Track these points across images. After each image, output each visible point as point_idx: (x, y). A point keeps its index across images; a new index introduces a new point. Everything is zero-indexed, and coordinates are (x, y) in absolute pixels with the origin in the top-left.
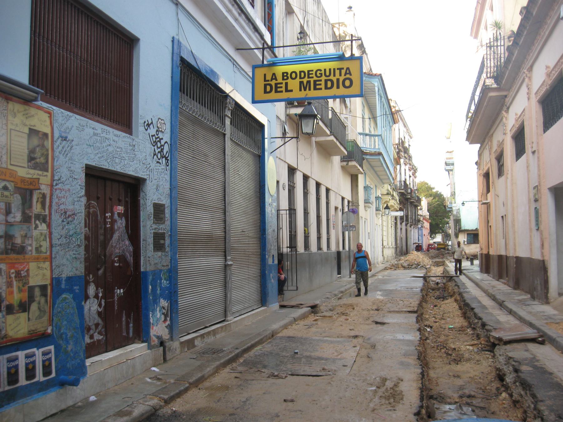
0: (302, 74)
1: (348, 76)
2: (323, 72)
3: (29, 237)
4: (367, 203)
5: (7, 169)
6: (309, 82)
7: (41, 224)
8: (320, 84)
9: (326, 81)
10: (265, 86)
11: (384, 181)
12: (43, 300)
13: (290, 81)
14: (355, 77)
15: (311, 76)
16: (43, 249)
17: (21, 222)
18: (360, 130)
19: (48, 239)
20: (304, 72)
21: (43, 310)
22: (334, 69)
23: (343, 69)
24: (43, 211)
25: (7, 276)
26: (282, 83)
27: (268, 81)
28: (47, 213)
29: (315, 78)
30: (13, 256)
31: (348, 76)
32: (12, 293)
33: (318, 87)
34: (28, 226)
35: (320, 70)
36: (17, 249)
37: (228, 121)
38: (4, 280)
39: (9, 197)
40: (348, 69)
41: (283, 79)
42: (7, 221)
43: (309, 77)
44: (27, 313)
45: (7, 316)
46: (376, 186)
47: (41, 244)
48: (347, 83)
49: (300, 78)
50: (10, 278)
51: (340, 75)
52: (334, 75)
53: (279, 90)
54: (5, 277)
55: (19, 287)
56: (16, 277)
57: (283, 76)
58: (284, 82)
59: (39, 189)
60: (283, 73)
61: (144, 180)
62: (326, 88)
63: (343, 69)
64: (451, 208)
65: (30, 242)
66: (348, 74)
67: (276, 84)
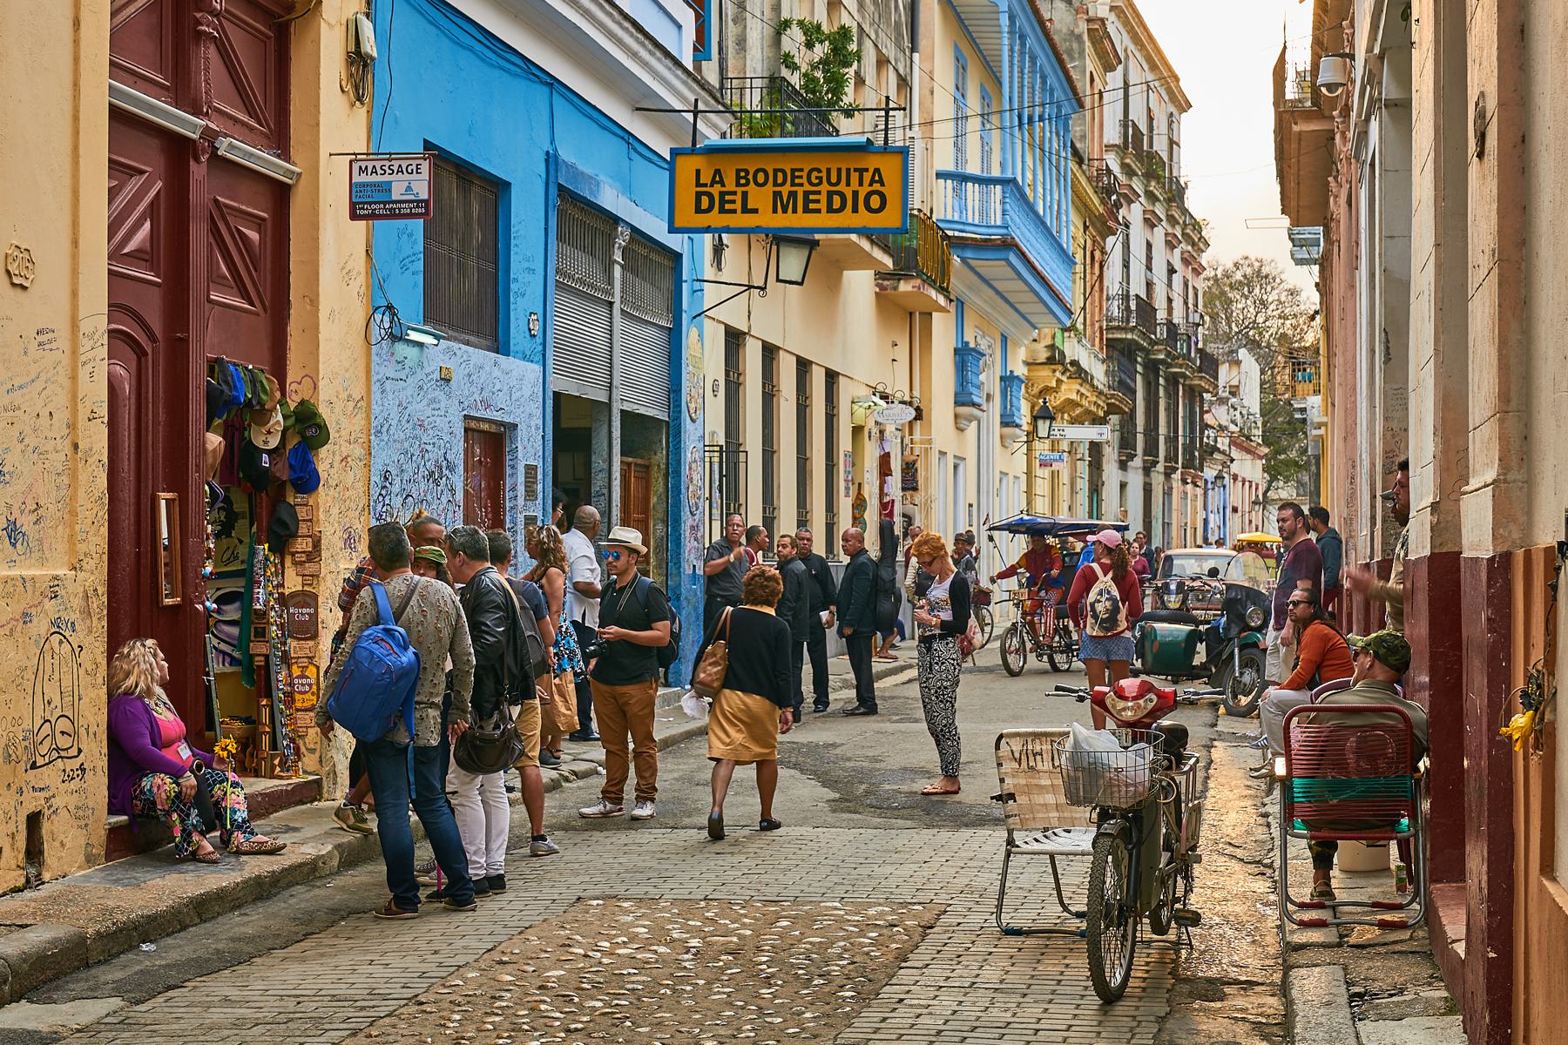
0: (780, 175)
1: (876, 187)
2: (824, 175)
4: (963, 404)
6: (793, 195)
8: (818, 201)
9: (830, 194)
10: (699, 195)
11: (1033, 319)
13: (752, 187)
14: (891, 190)
15: (797, 181)
18: (945, 160)
20: (783, 171)
22: (848, 170)
23: (867, 170)
26: (735, 193)
27: (705, 185)
29: (807, 187)
31: (876, 187)
33: (812, 206)
35: (819, 171)
37: (617, 271)
40: (877, 170)
41: (738, 184)
43: (793, 184)
46: (1004, 339)
48: (875, 202)
49: (775, 184)
51: (861, 184)
52: (848, 184)
53: (727, 206)
57: (738, 178)
58: (740, 189)
60: (738, 171)
61: (515, 426)
62: (830, 210)
63: (867, 170)
64: (1303, 410)
66: (877, 182)
67: (722, 194)
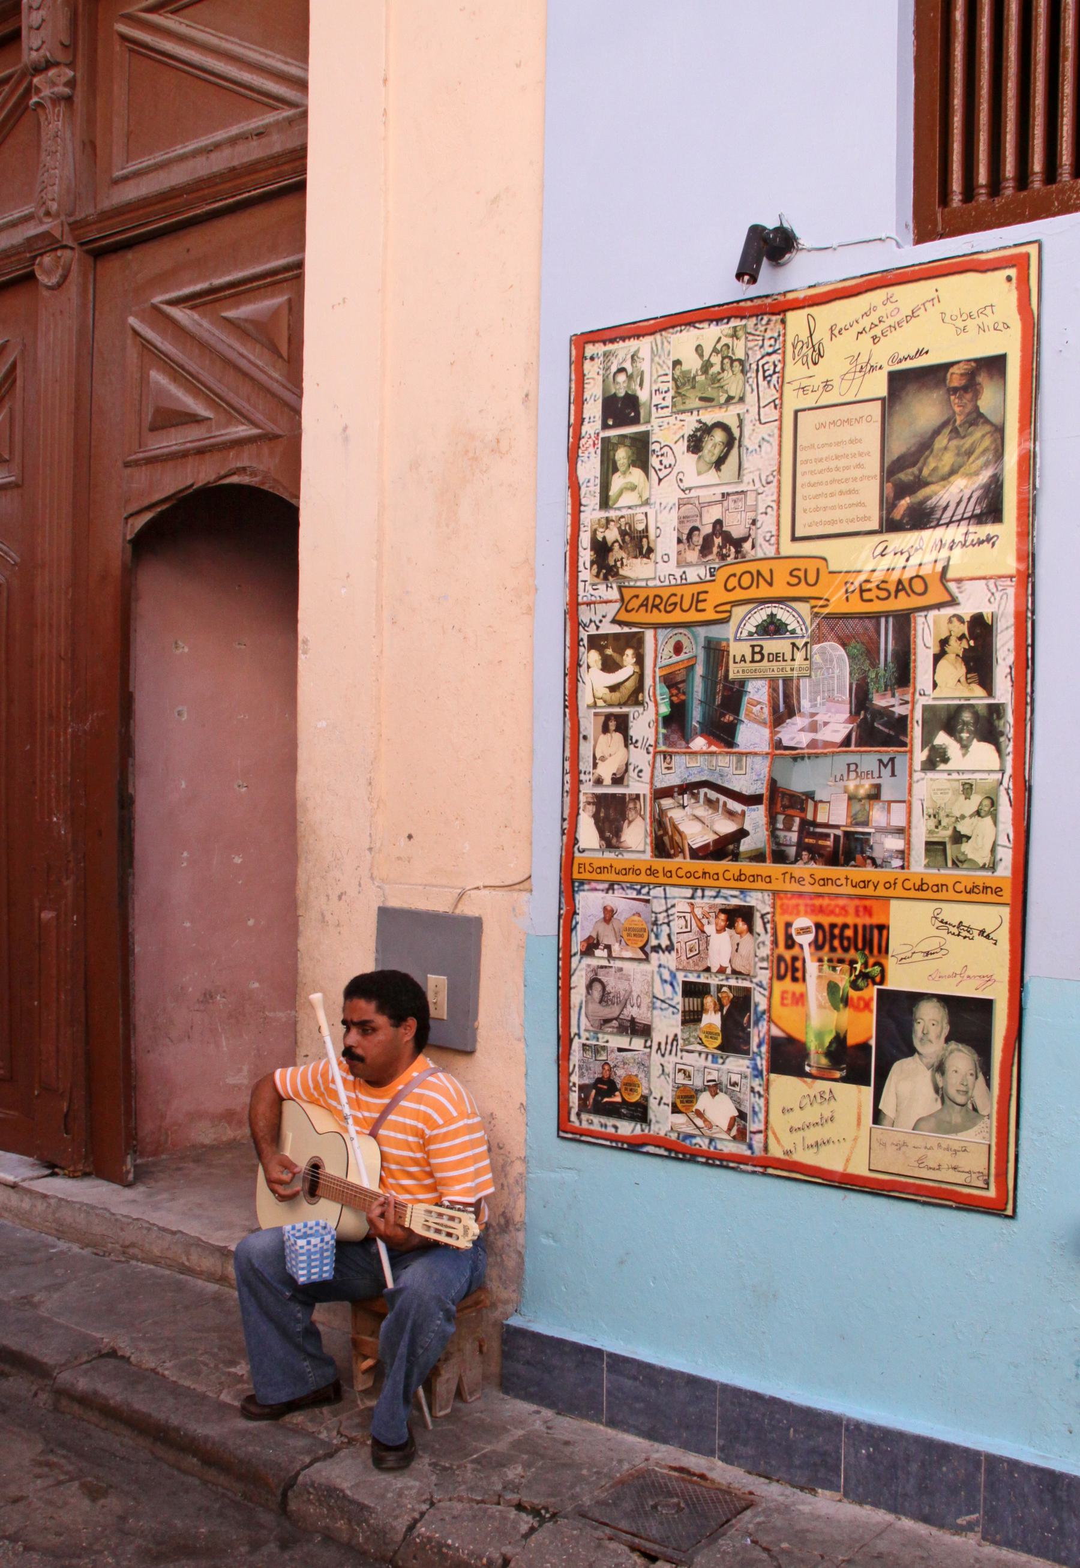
3: (890, 802)
5: (778, 558)
7: (965, 747)
12: (962, 1060)
16: (976, 851)
17: (847, 742)
19: (1005, 811)
21: (960, 1099)
24: (979, 691)
25: (775, 934)
28: (1004, 691)
30: (807, 869)
32: (800, 999)
34: (885, 759)
36: (829, 843)
38: (765, 951)
39: (788, 657)
42: (778, 745)
44: (868, 1091)
45: (773, 1076)
47: (963, 828)
50: (790, 943)
54: (767, 939)
55: (832, 988)
56: (817, 946)
59: (953, 602)
65: (898, 818)
